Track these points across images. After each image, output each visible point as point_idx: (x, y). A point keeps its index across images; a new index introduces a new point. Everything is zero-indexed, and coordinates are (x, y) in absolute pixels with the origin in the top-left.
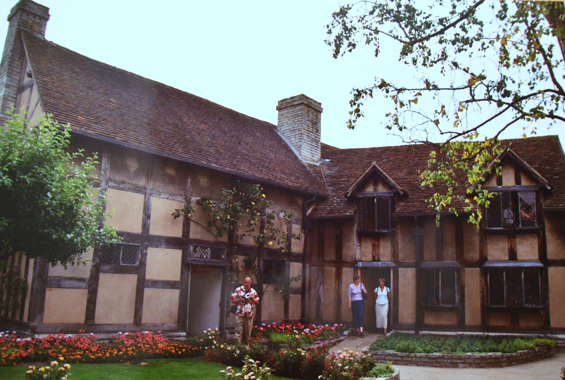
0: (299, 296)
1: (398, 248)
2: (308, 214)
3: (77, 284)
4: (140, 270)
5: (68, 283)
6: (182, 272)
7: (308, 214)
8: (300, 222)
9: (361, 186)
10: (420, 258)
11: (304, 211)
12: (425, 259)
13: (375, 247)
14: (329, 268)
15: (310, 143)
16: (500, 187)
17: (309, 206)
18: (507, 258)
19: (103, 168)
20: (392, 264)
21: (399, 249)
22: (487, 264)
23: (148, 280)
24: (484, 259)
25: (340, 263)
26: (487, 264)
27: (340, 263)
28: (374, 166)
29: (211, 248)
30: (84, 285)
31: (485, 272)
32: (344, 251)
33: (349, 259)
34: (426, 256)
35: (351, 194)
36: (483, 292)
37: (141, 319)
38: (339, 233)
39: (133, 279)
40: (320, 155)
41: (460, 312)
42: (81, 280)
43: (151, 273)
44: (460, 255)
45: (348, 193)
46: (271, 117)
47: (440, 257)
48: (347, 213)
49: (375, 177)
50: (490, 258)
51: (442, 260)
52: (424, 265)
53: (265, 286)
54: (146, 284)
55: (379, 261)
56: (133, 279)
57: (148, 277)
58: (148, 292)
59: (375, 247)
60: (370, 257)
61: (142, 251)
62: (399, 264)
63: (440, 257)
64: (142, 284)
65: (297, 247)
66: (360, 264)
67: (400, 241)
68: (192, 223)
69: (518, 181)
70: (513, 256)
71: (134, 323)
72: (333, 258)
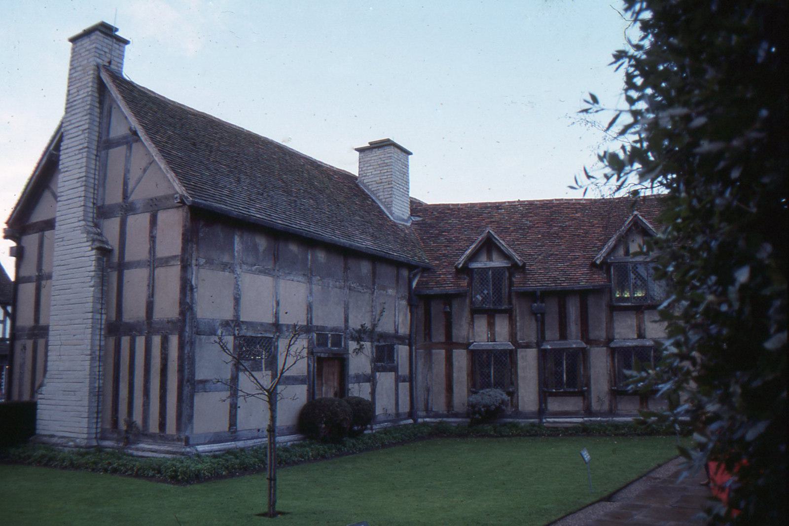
0: (407, 384)
1: (516, 326)
9: (473, 257)
10: (541, 338)
12: (546, 339)
13: (491, 325)
14: (438, 351)
18: (636, 337)
19: (236, 249)
21: (518, 328)
22: (612, 345)
24: (610, 339)
25: (450, 344)
26: (612, 345)
27: (450, 344)
28: (489, 232)
31: (613, 352)
32: (455, 332)
33: (461, 341)
34: (548, 335)
35: (463, 265)
36: (610, 374)
38: (449, 310)
40: (409, 213)
41: (584, 395)
44: (585, 334)
45: (460, 263)
46: (351, 165)
47: (563, 336)
49: (489, 246)
50: (617, 336)
59: (491, 325)
60: (485, 337)
63: (563, 336)
65: (404, 330)
67: (518, 319)
70: (641, 336)
72: (442, 339)
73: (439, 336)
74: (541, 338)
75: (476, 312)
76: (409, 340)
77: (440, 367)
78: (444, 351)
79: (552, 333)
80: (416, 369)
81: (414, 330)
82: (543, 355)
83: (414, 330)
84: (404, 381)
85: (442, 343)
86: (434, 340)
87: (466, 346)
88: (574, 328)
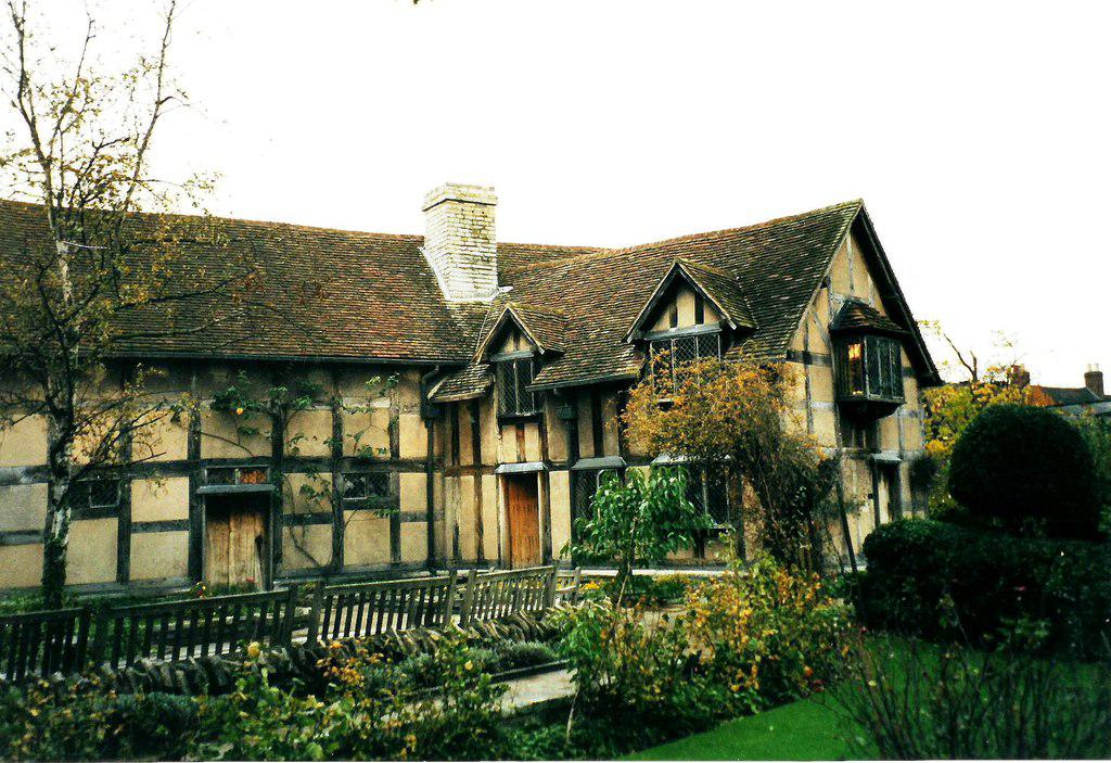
0: (424, 525)
2: (430, 395)
3: (28, 538)
4: (122, 509)
5: (13, 539)
6: (192, 508)
7: (430, 395)
8: (417, 409)
11: (423, 394)
13: (520, 438)
15: (469, 265)
16: (673, 329)
17: (431, 382)
20: (539, 466)
23: (136, 523)
25: (478, 468)
27: (478, 468)
29: (240, 469)
30: (38, 538)
32: (483, 450)
34: (582, 452)
37: (128, 575)
39: (110, 526)
42: (35, 532)
43: (139, 513)
44: (624, 450)
47: (599, 453)
48: (477, 390)
51: (603, 456)
52: (579, 465)
53: (347, 514)
54: (133, 528)
55: (525, 462)
56: (110, 526)
57: (134, 519)
58: (135, 538)
59: (520, 438)
61: (122, 486)
62: (550, 465)
64: (126, 530)
66: (501, 470)
68: (203, 438)
69: (699, 319)
71: (118, 580)
73: (467, 458)
74: (574, 455)
75: (503, 422)
76: (428, 466)
77: (469, 499)
78: (472, 477)
79: (586, 448)
80: (444, 502)
81: (436, 450)
82: (575, 477)
83: (436, 450)
84: (415, 518)
85: (471, 467)
86: (463, 463)
87: (493, 469)
88: (611, 441)
